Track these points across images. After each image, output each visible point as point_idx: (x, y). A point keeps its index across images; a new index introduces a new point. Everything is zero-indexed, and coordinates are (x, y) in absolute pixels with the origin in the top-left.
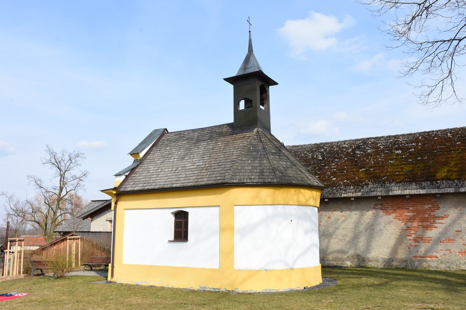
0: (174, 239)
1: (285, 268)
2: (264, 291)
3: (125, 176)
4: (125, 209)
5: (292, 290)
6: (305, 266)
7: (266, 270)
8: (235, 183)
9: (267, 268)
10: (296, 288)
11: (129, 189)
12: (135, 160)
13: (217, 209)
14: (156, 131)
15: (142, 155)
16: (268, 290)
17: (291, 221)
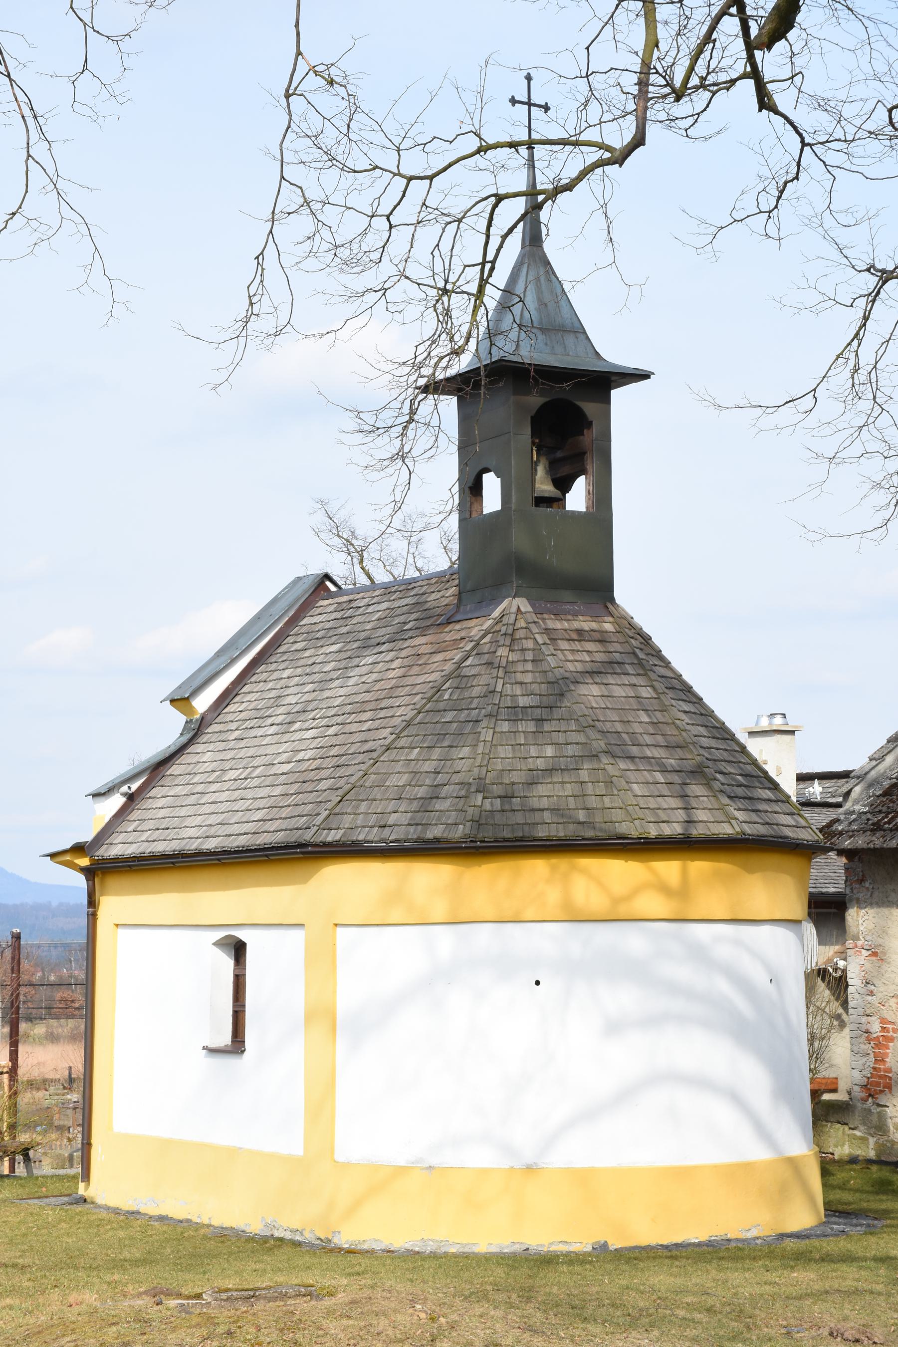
0: (232, 1041)
1: (505, 1164)
2: (416, 1245)
3: (124, 794)
4: (117, 925)
5: (527, 1249)
6: (603, 1160)
7: (431, 1168)
8: (330, 844)
9: (434, 1162)
10: (552, 1244)
11: (130, 850)
12: (187, 722)
13: (298, 935)
14: (299, 579)
15: (202, 703)
16: (431, 1243)
17: (537, 983)
